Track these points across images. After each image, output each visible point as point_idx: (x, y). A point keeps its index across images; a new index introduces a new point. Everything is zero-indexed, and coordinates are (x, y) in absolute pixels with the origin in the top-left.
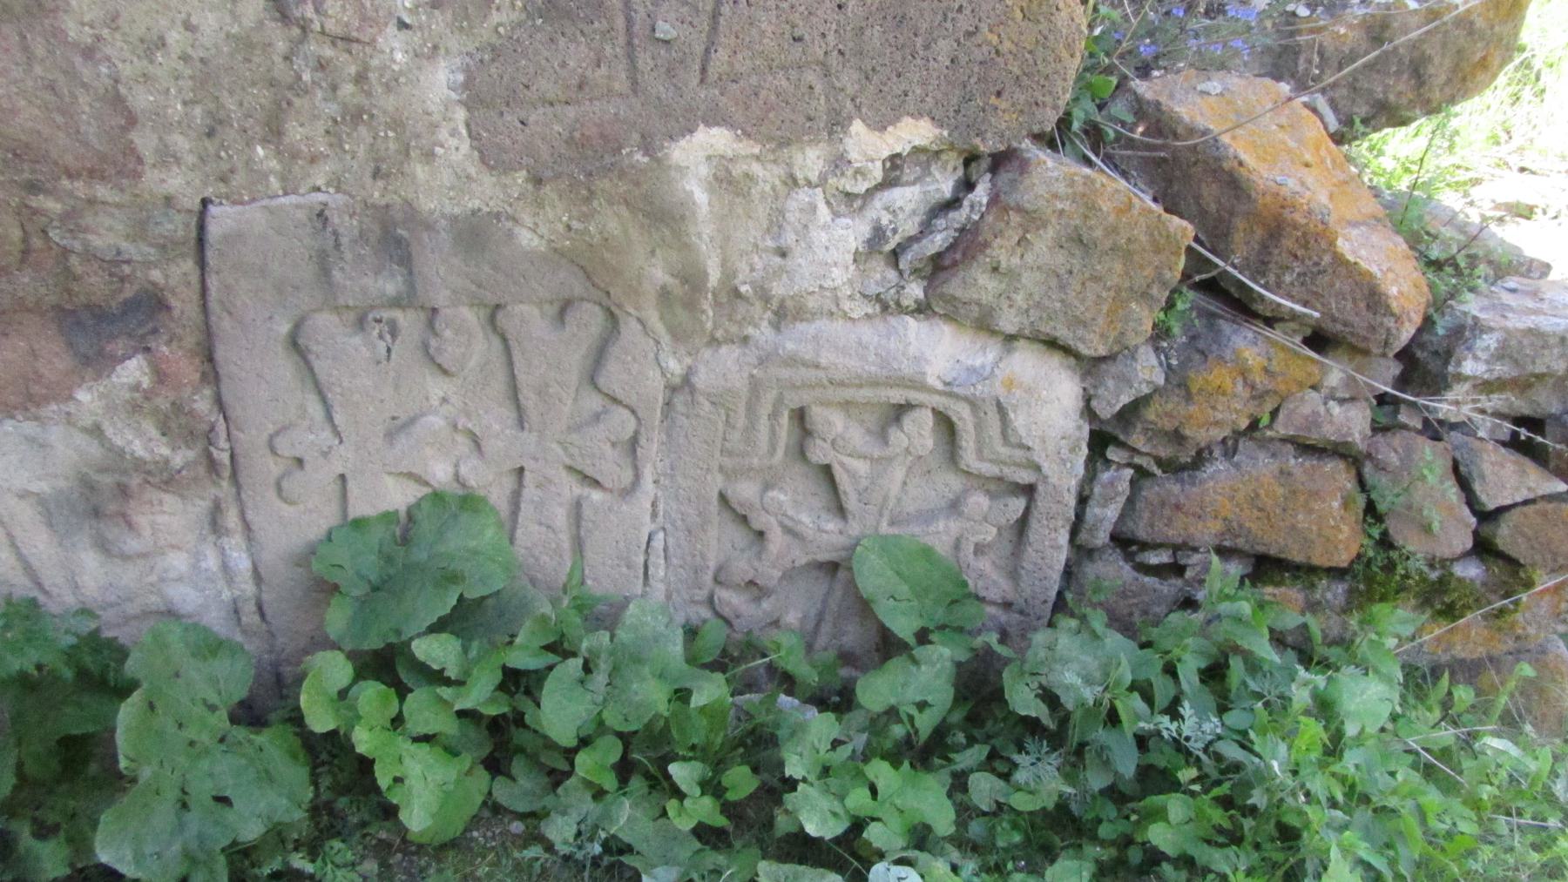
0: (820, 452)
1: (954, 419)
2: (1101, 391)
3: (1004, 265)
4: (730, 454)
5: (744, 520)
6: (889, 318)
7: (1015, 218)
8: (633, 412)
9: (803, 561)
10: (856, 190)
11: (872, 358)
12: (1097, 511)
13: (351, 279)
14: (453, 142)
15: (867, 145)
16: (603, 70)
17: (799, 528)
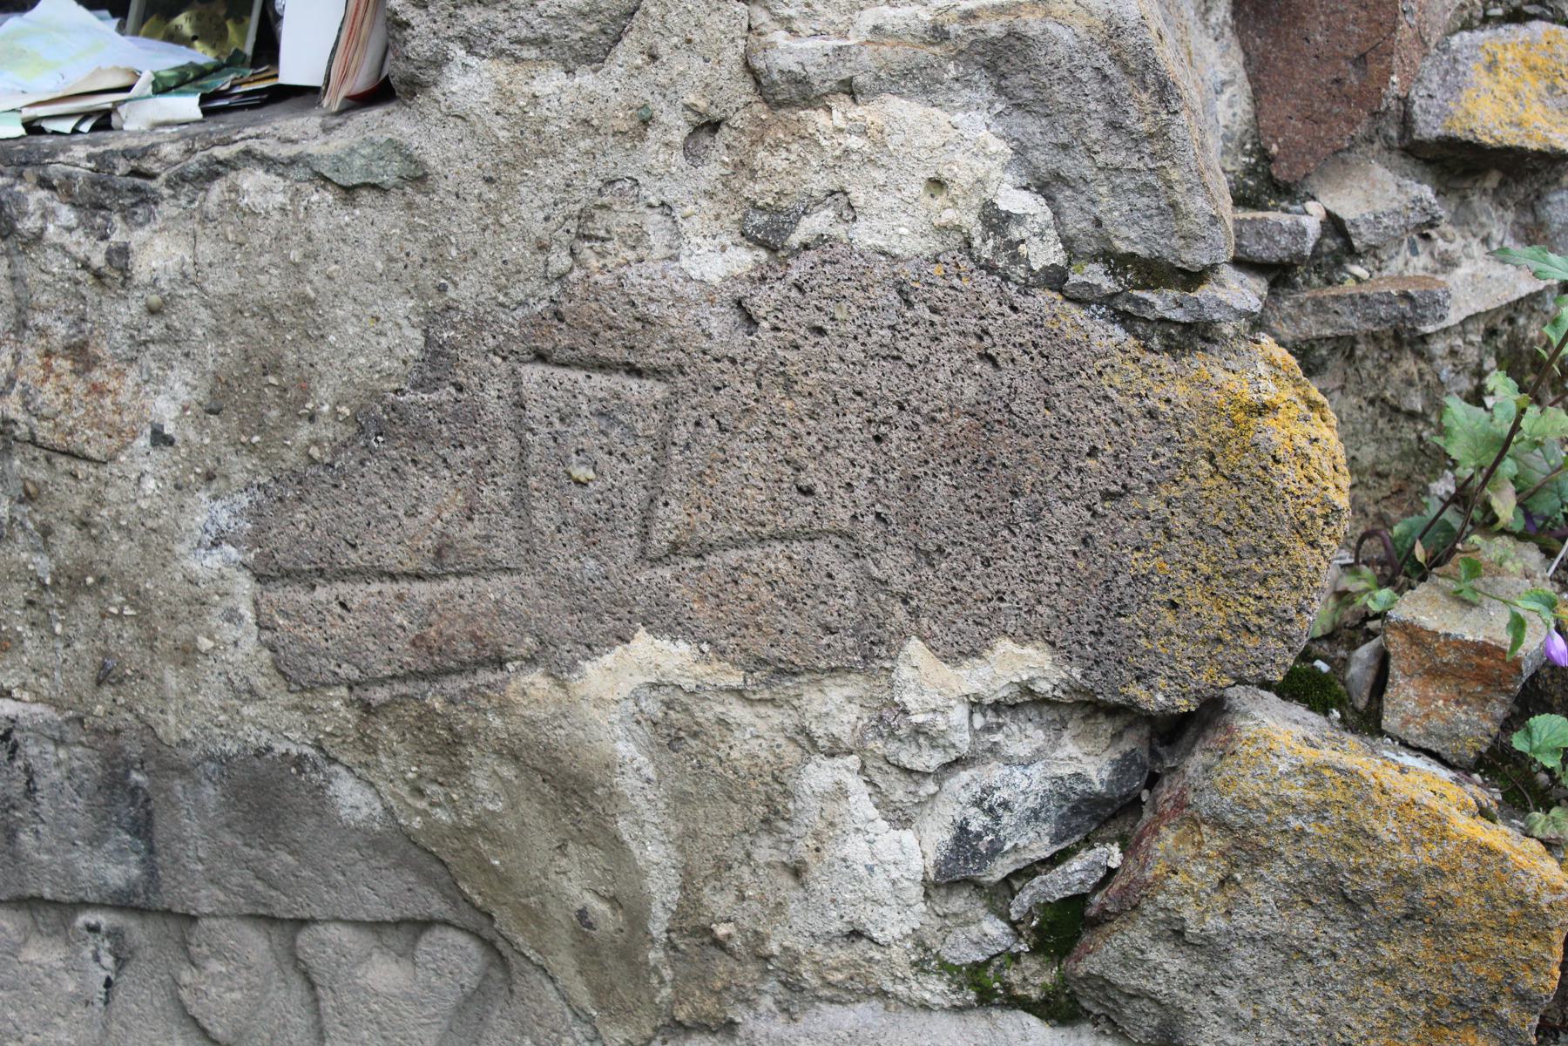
3: (1193, 928)
6: (996, 1013)
7: (1216, 843)
10: (918, 765)
13: (50, 851)
14: (229, 632)
15: (931, 683)
16: (476, 527)
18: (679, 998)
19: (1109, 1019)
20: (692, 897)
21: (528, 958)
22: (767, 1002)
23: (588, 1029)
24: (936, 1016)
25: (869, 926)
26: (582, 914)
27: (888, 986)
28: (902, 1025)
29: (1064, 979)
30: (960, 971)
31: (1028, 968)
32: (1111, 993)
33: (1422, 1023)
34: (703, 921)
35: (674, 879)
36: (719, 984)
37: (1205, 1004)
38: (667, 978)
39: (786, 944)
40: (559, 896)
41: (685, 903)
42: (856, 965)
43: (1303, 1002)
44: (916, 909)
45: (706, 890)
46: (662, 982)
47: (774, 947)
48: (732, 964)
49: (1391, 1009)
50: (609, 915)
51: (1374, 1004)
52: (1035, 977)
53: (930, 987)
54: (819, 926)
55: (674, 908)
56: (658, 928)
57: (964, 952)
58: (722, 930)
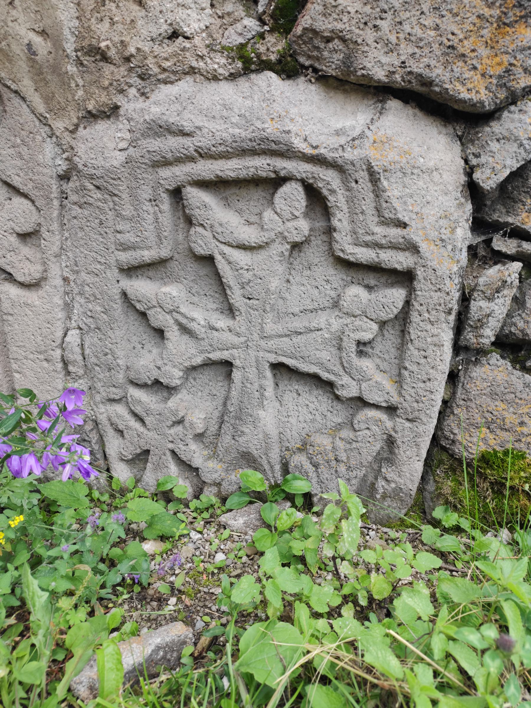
0: (203, 242)
1: (325, 192)
2: (483, 159)
4: (125, 247)
5: (143, 315)
6: (253, 76)
8: (33, 202)
9: (198, 360)
11: (235, 119)
12: (483, 304)
17: (193, 326)
18: (89, 95)
19: (315, 70)
20: (86, 25)
21: (9, 87)
22: (133, 91)
23: (47, 128)
24: (222, 83)
25: (182, 24)
26: (29, 45)
27: (194, 64)
28: (204, 92)
29: (290, 46)
30: (233, 50)
31: (269, 41)
32: (317, 42)
33: (495, 25)
34: (94, 42)
35: (73, 12)
36: (106, 83)
37: (370, 35)
38: (80, 84)
39: (139, 46)
40: (16, 37)
41: (82, 30)
42: (176, 55)
43: (426, 23)
44: (206, 11)
45: (93, 20)
46: (77, 85)
47: (132, 50)
48: (112, 67)
49: (479, 17)
50: (43, 43)
51: (469, 15)
52: (273, 46)
53: (217, 60)
54: (155, 31)
55: (77, 33)
56: (70, 47)
57: (233, 38)
58: (103, 45)
